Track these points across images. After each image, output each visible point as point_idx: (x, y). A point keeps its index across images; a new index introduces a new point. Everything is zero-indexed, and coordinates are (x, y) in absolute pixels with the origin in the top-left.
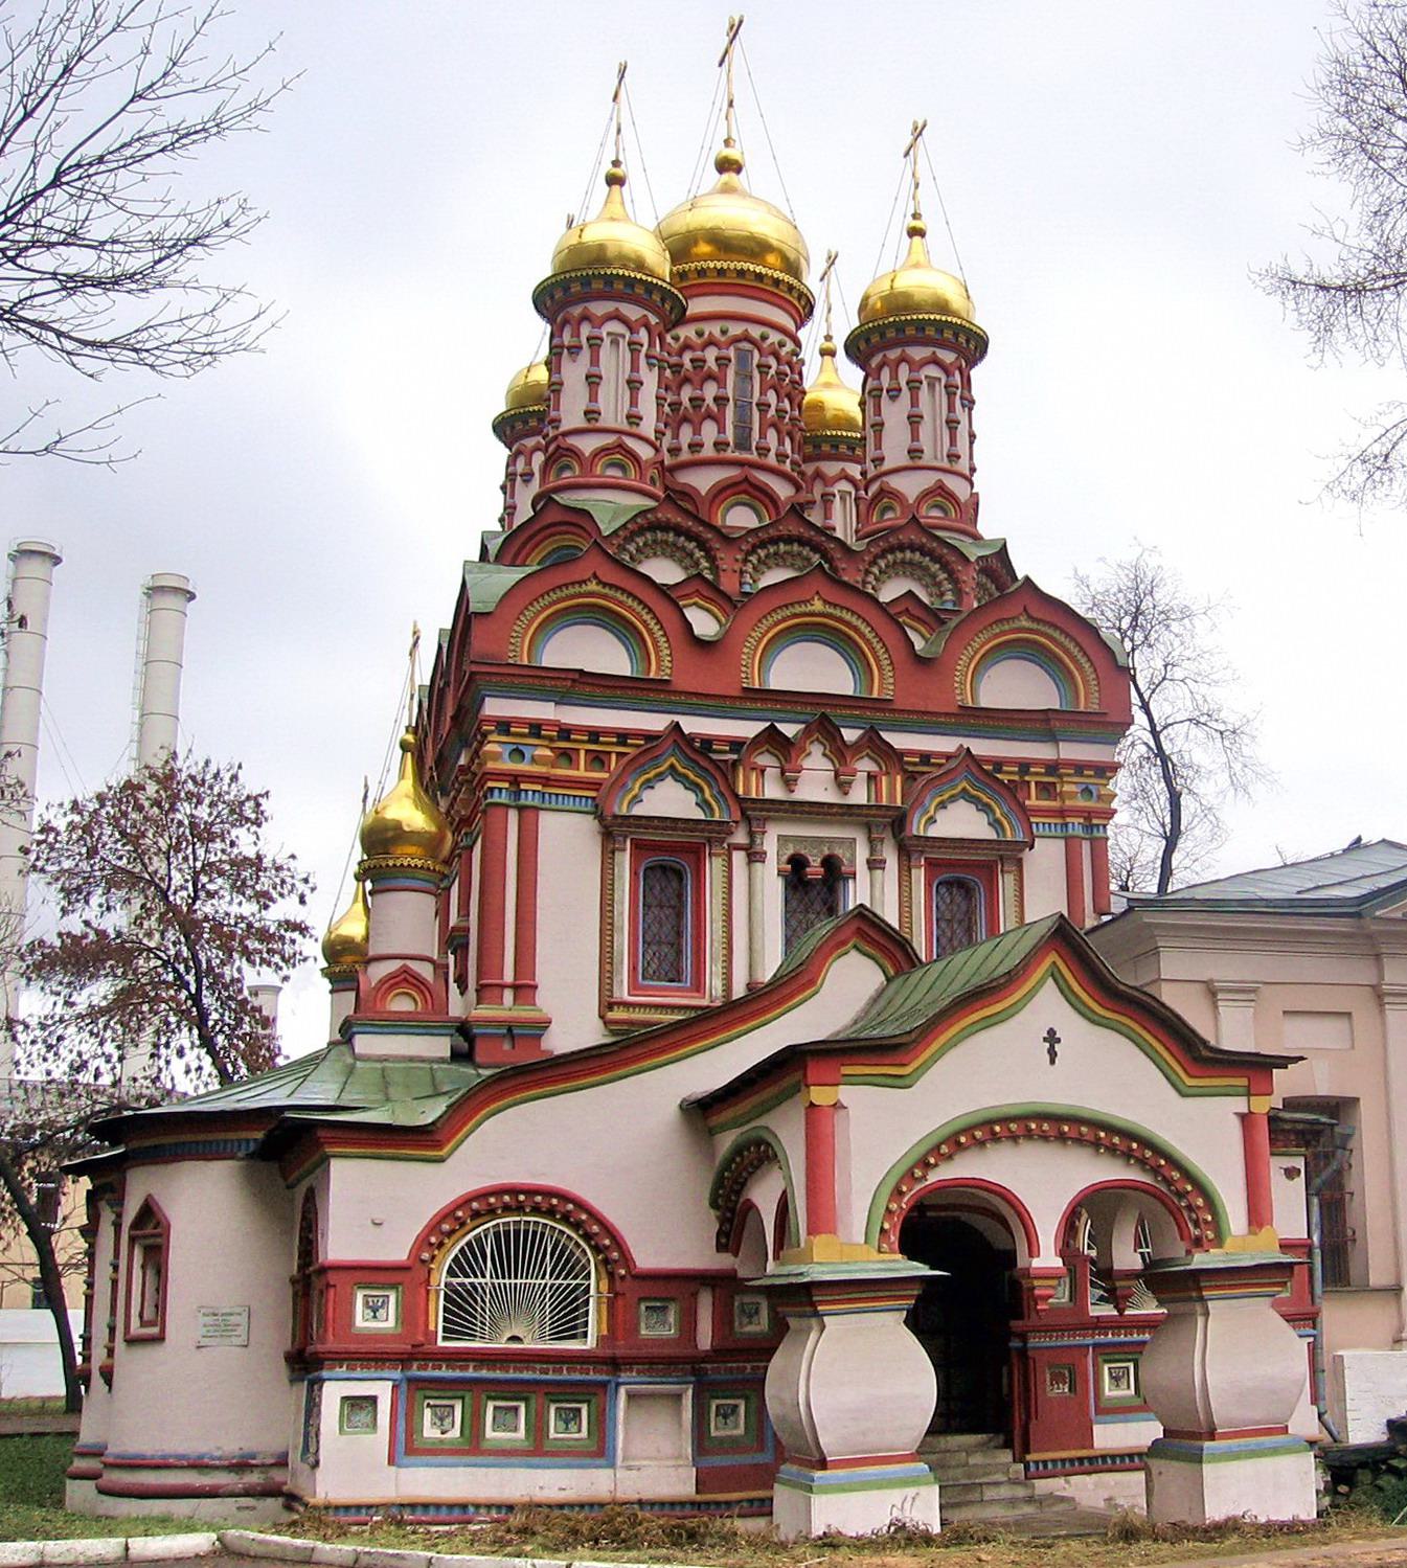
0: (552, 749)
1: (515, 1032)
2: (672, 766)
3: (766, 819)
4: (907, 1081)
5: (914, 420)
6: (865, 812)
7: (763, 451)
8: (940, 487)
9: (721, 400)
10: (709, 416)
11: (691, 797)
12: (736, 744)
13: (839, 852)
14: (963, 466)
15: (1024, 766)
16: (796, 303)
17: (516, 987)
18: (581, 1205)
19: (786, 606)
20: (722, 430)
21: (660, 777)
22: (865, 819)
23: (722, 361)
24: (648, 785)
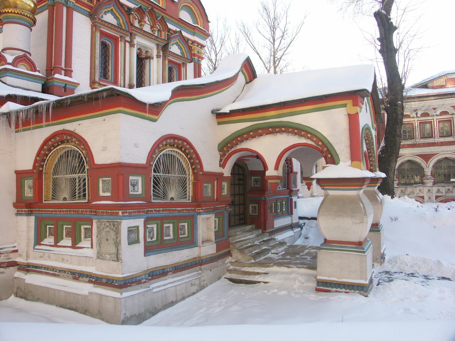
1: (67, 86)
2: (112, 10)
12: (130, 9)
13: (149, 51)
17: (65, 70)
18: (192, 147)
22: (158, 43)
24: (105, 13)
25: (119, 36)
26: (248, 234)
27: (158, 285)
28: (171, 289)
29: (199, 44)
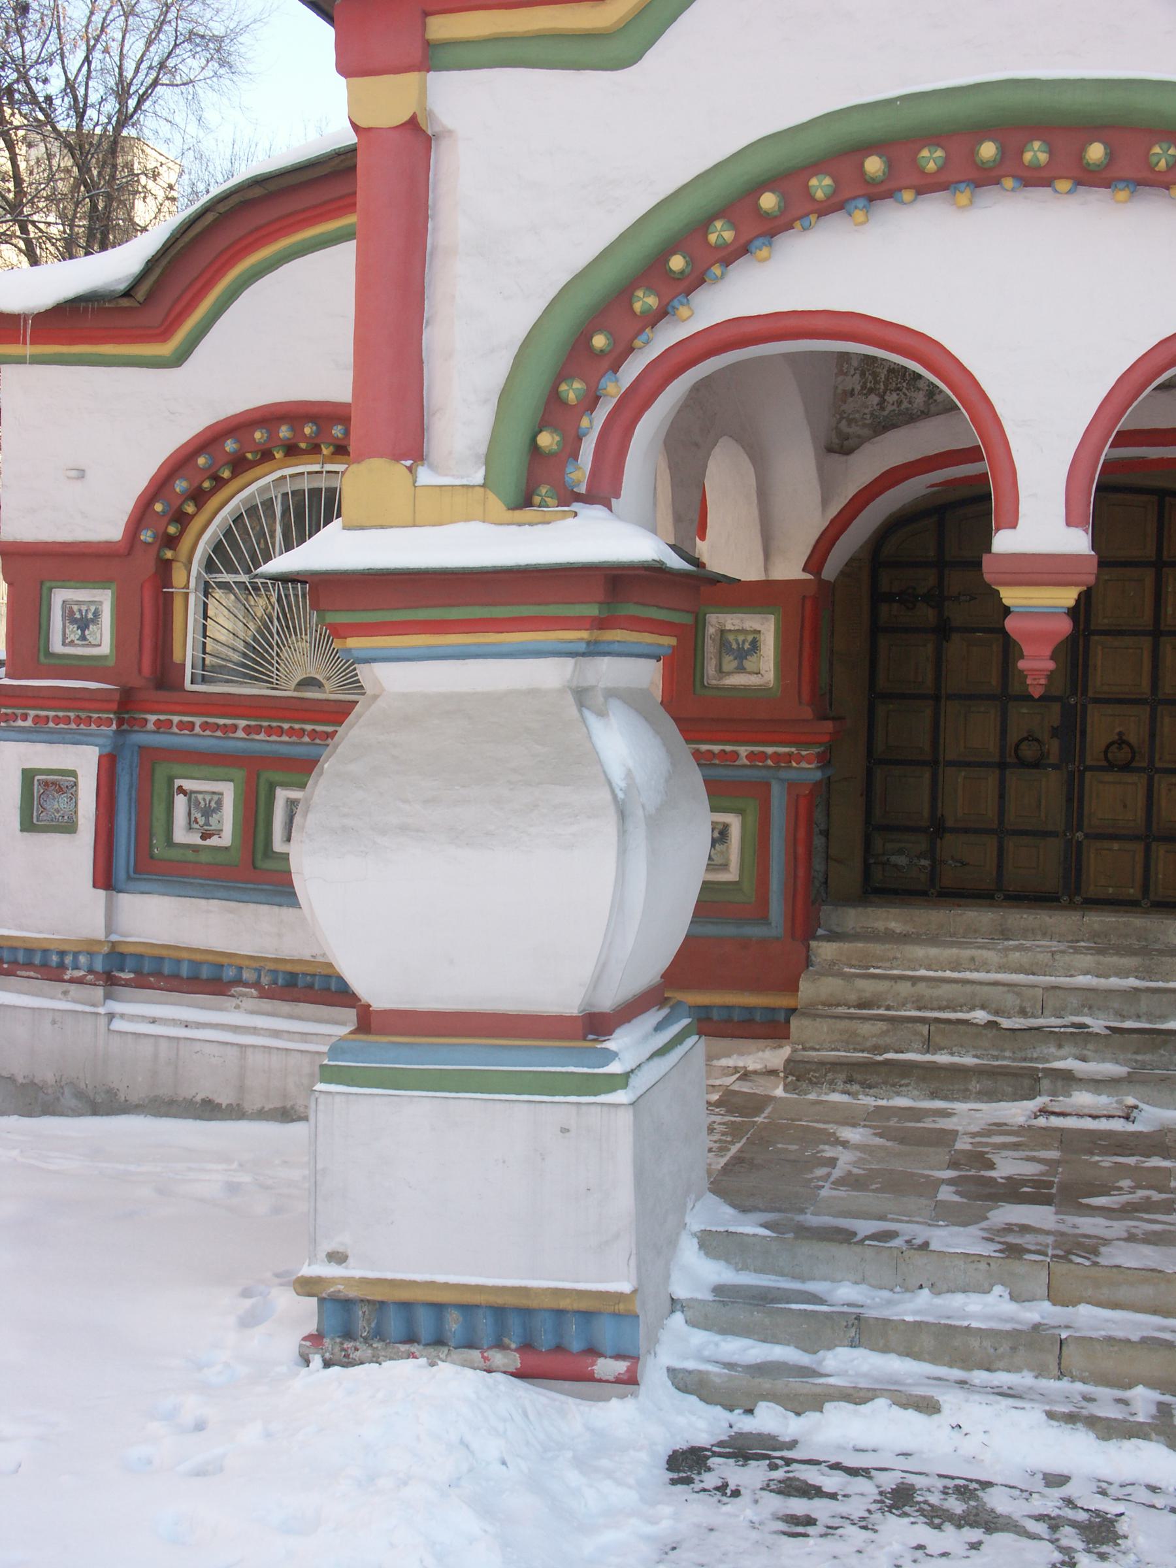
26: (1088, 960)
27: (147, 1015)
28: (208, 1049)
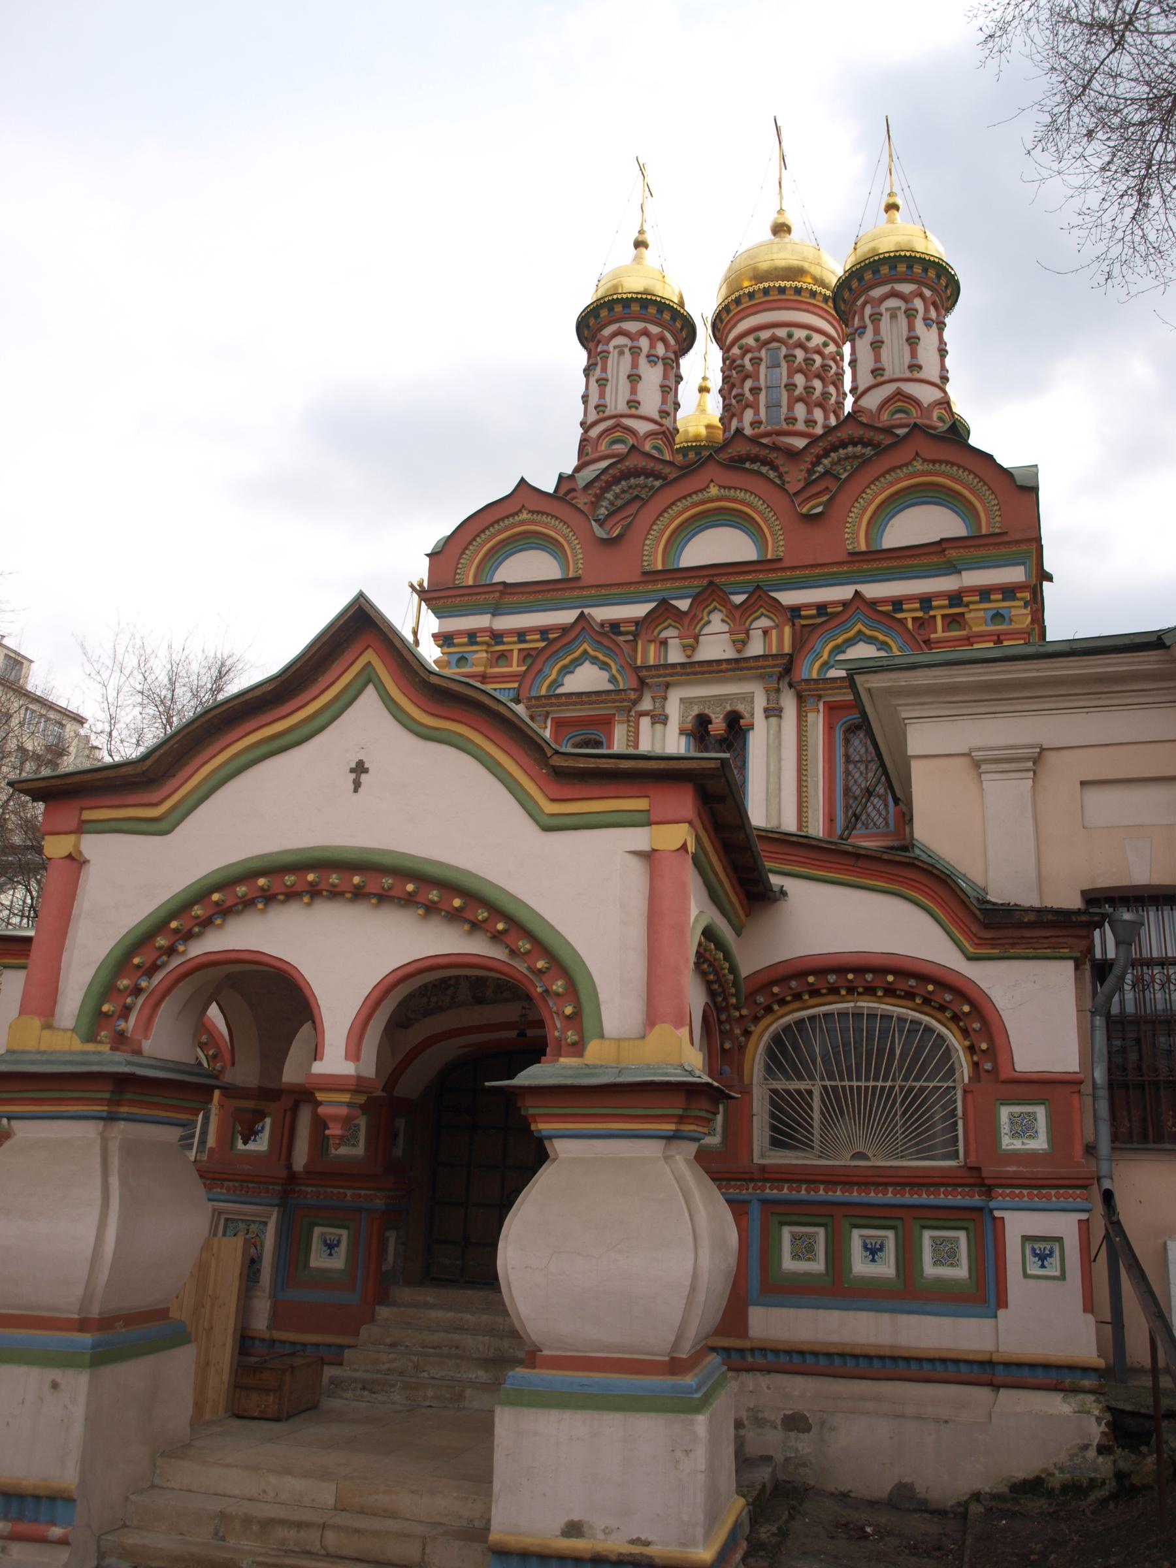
0: (487, 652)
2: (585, 652)
3: (667, 686)
4: (163, 826)
5: (877, 345)
6: (752, 664)
7: (792, 420)
8: (899, 393)
9: (755, 390)
10: (748, 406)
11: (605, 675)
12: (637, 622)
13: (740, 707)
14: (931, 371)
15: (925, 601)
16: (824, 306)
19: (685, 497)
20: (757, 413)
21: (577, 662)
23: (756, 361)
24: (567, 670)
25: (612, 712)
29: (985, 593)
